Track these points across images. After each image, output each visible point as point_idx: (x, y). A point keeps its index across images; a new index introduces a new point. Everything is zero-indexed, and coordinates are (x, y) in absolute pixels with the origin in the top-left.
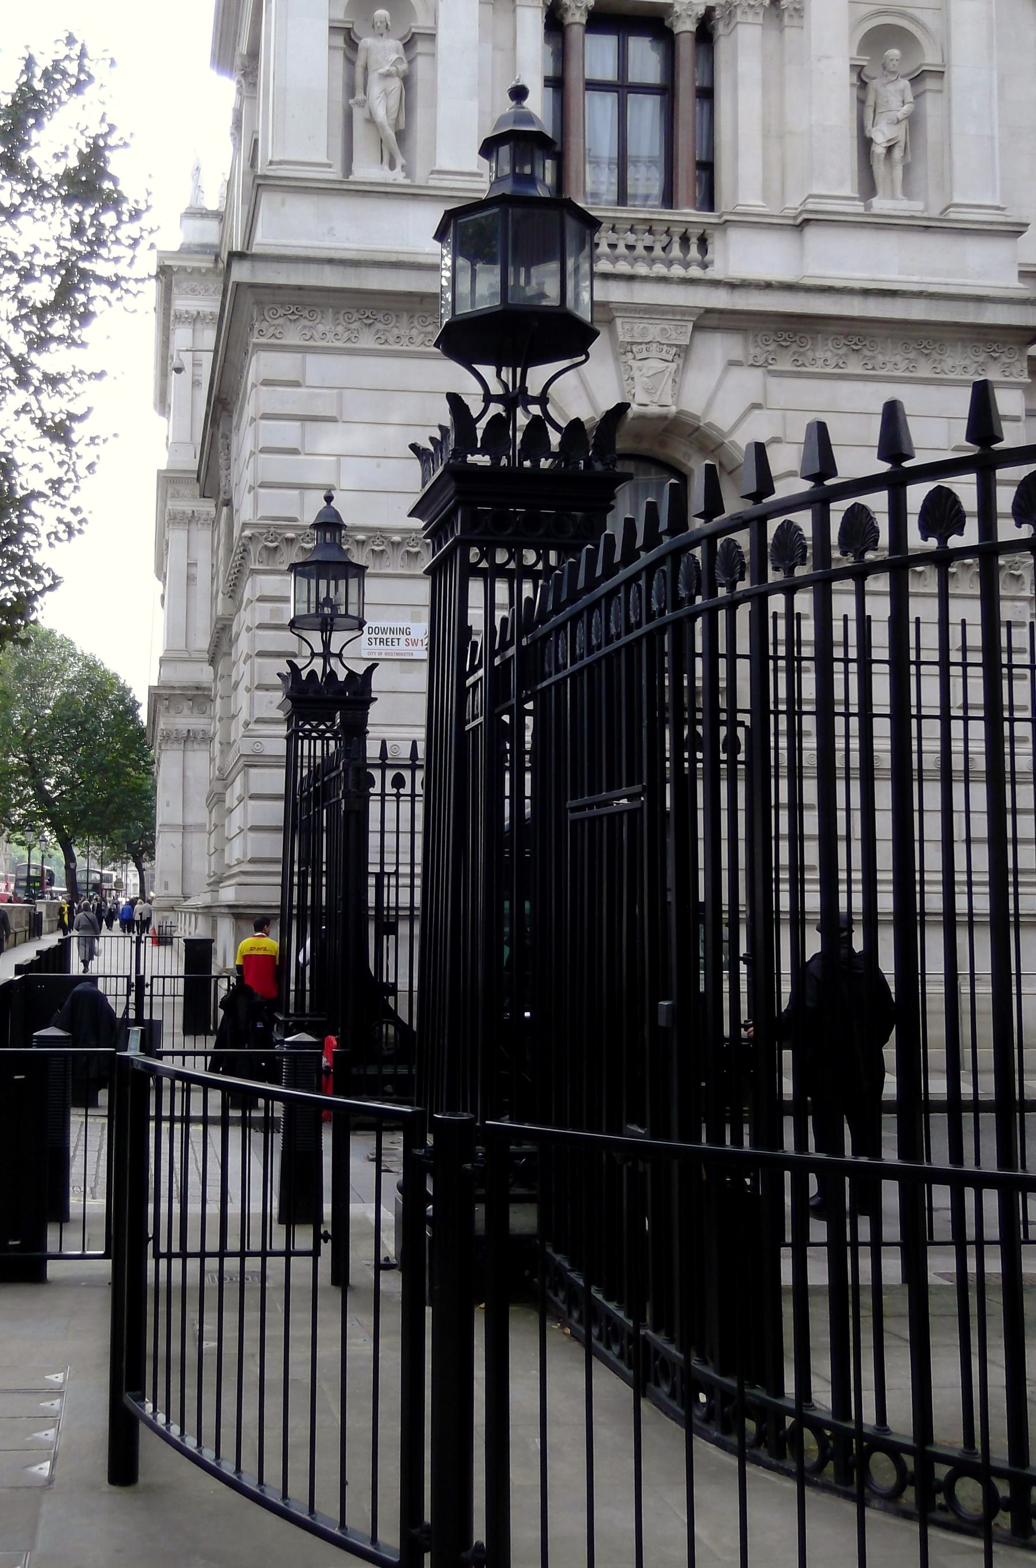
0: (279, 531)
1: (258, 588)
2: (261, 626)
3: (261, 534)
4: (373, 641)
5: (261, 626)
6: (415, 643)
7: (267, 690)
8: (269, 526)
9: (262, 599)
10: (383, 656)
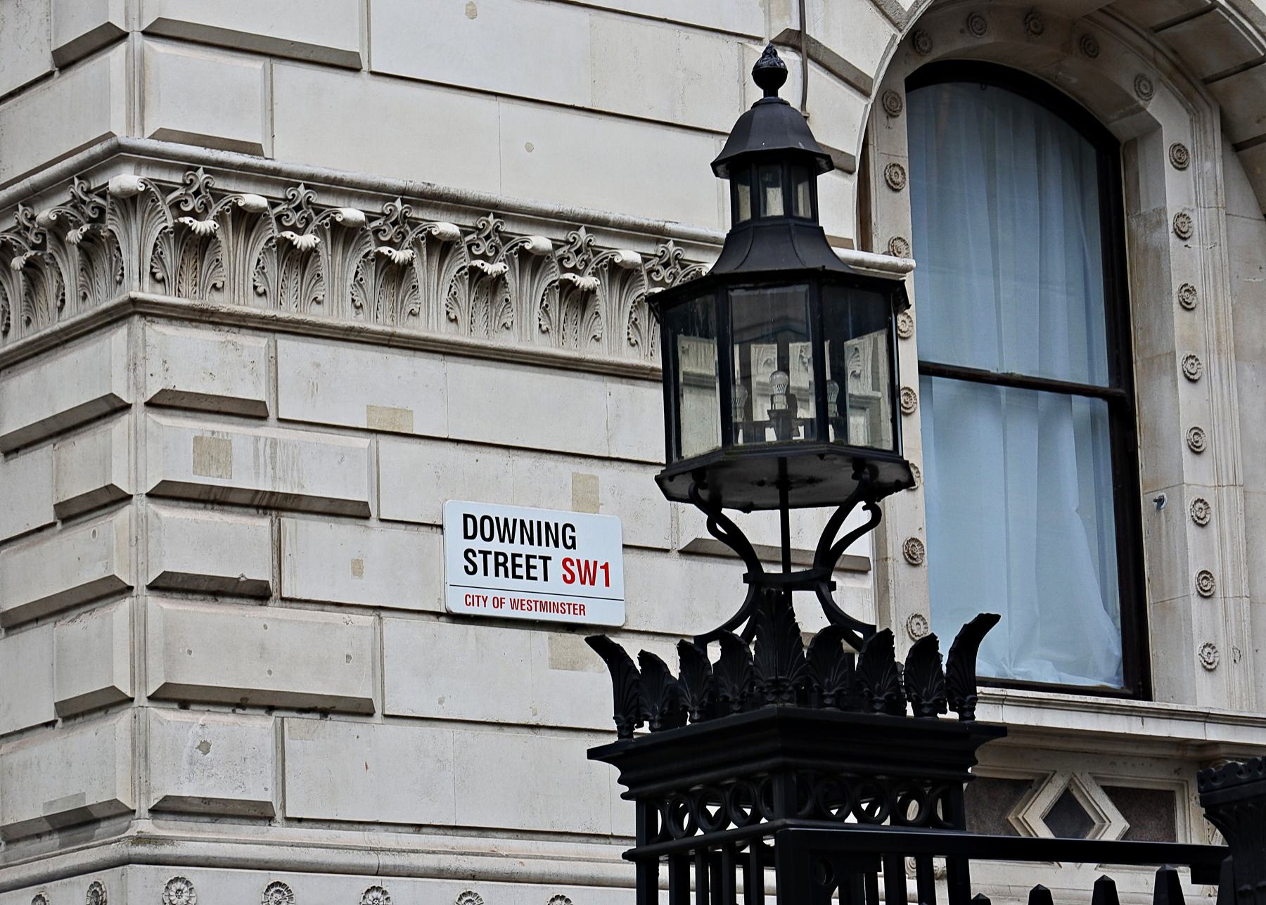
0: (219, 184)
1: (154, 365)
2: (166, 493)
3: (166, 189)
4: (479, 560)
5: (166, 493)
6: (587, 573)
7: (184, 705)
8: (190, 165)
9: (165, 403)
10: (506, 612)
